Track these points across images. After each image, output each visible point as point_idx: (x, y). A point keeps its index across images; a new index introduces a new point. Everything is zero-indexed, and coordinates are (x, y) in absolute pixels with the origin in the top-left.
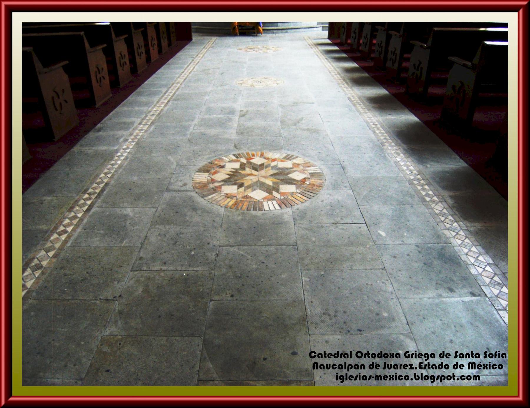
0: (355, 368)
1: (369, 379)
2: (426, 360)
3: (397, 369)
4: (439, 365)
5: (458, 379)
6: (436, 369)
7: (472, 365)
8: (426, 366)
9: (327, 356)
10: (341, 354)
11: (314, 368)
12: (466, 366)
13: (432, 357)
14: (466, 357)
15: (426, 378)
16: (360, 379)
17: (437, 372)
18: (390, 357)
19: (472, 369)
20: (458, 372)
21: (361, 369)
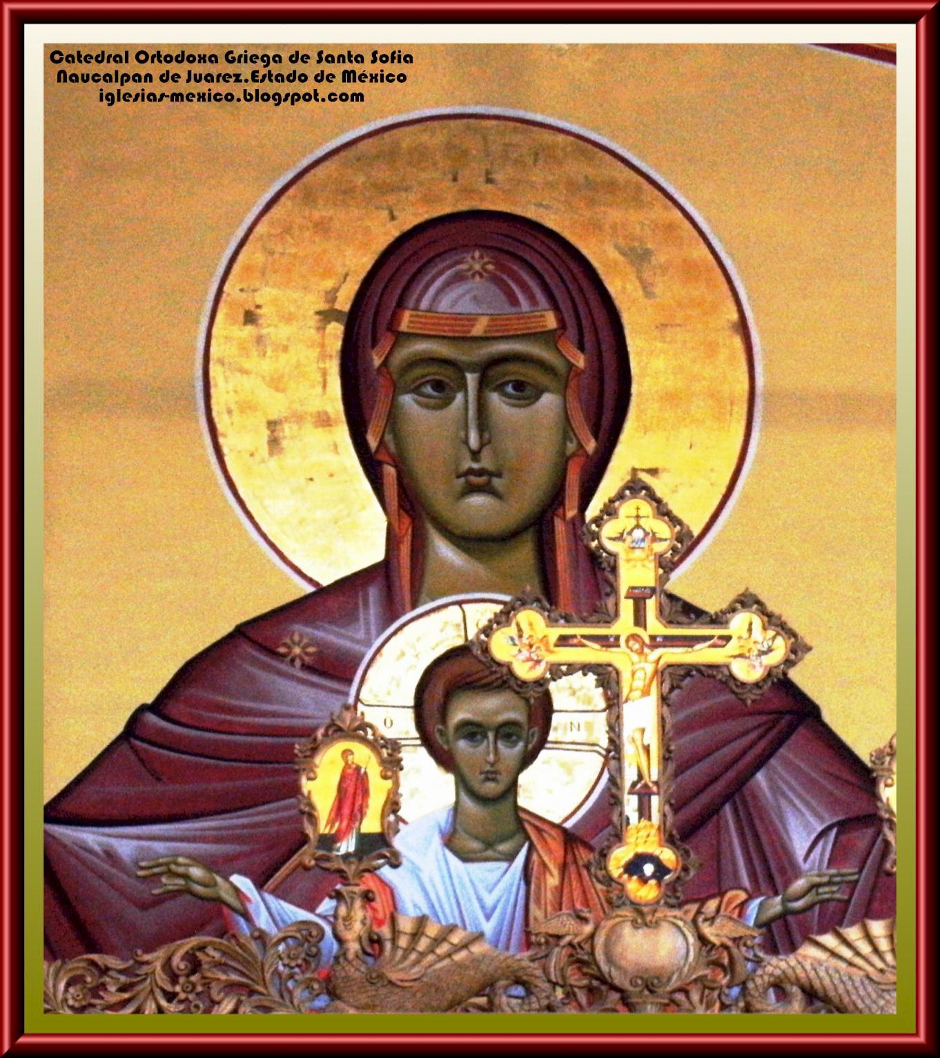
0: (135, 80)
1: (160, 100)
2: (265, 66)
3: (212, 81)
4: (289, 76)
5: (323, 100)
6: (283, 81)
7: (348, 76)
8: (264, 76)
9: (82, 59)
10: (110, 56)
11: (59, 80)
12: (339, 77)
13: (276, 62)
14: (339, 62)
15: (266, 97)
16: (143, 100)
17: (285, 88)
18: (199, 62)
19: (349, 81)
20: (324, 89)
21: (146, 81)
